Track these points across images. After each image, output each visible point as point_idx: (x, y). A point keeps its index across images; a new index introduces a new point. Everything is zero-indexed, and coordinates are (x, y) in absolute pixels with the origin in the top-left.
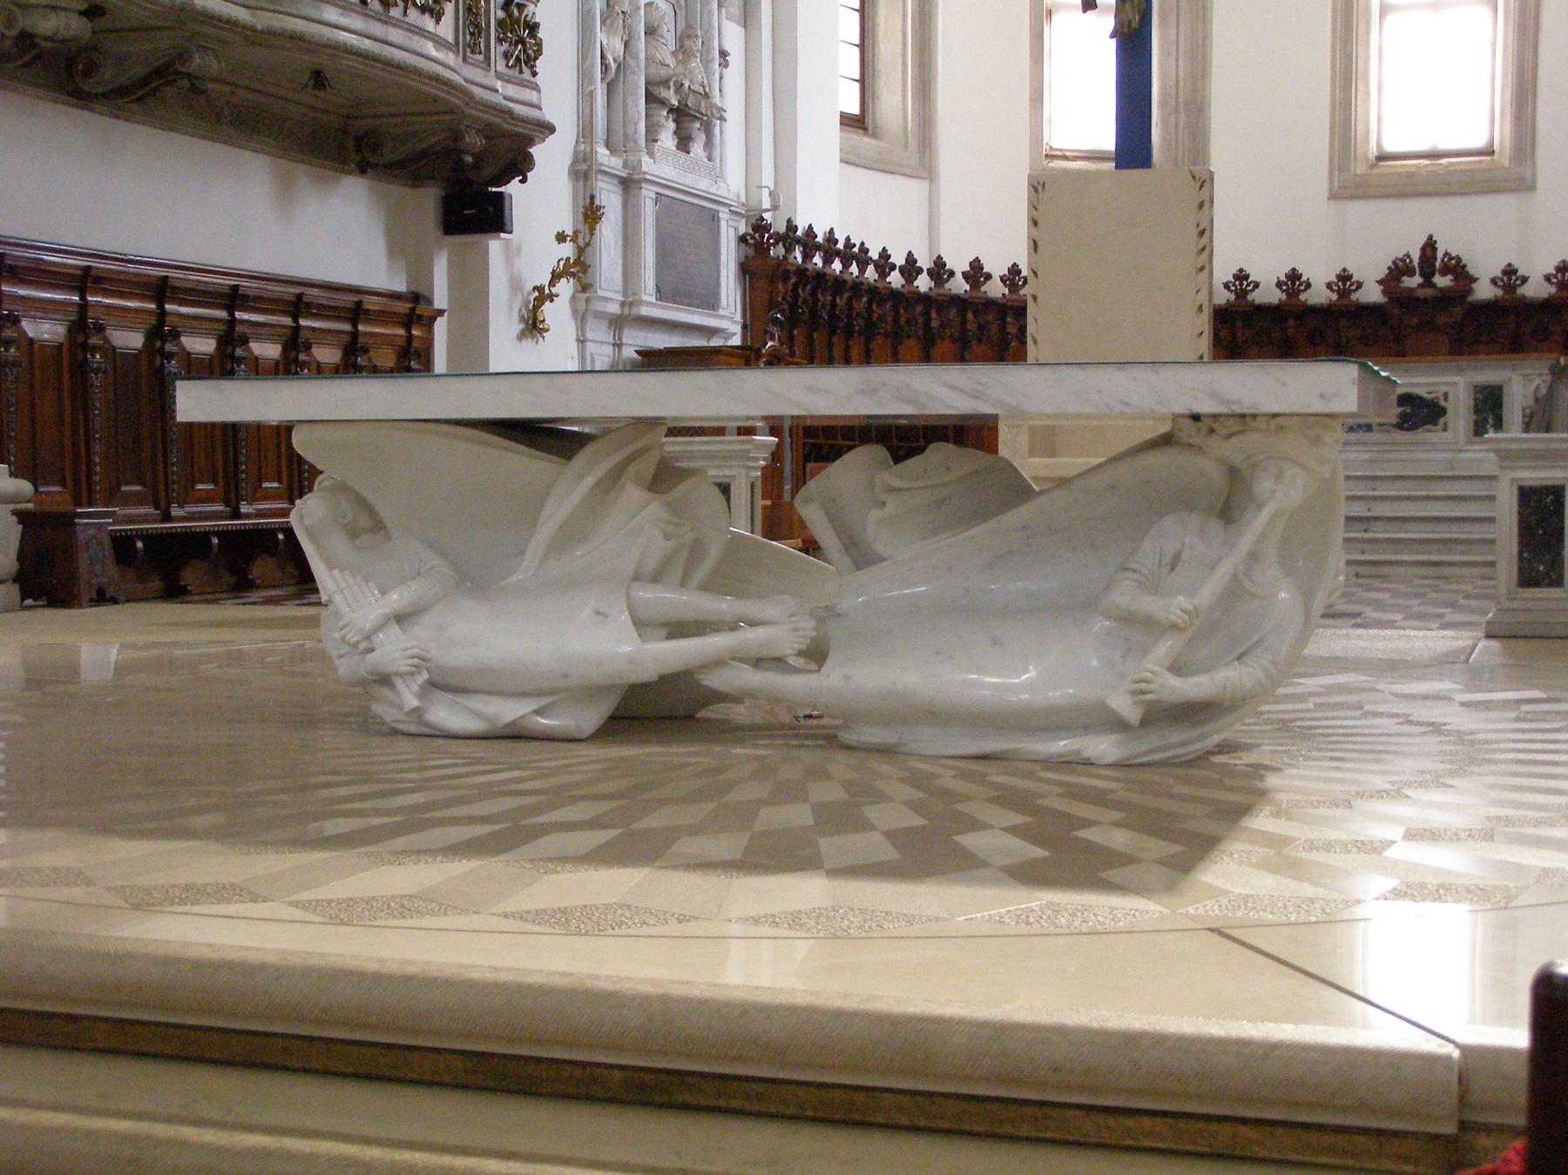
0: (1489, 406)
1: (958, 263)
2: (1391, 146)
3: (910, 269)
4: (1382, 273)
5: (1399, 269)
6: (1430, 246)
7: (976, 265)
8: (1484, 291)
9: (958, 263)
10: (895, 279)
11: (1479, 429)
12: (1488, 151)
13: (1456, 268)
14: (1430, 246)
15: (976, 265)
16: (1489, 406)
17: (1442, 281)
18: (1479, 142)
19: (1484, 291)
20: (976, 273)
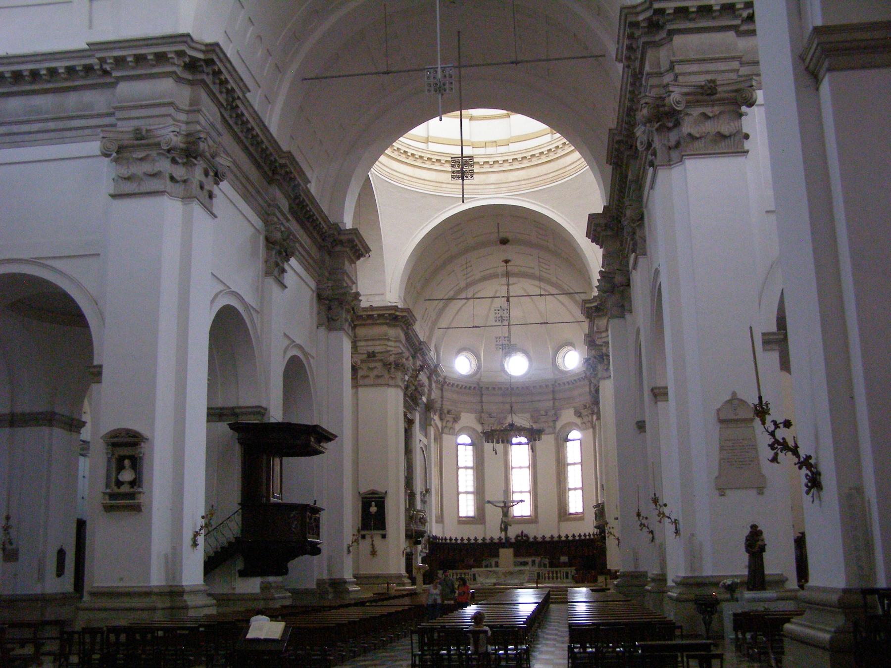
0: (534, 562)
1: (448, 538)
2: (515, 515)
3: (442, 539)
4: (515, 537)
5: (517, 536)
6: (522, 532)
7: (451, 538)
8: (531, 540)
9: (448, 538)
10: (444, 541)
11: (533, 565)
12: (530, 516)
13: (526, 536)
14: (522, 532)
15: (451, 538)
16: (534, 562)
17: (524, 538)
18: (529, 514)
19: (531, 540)
20: (451, 539)
